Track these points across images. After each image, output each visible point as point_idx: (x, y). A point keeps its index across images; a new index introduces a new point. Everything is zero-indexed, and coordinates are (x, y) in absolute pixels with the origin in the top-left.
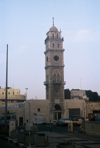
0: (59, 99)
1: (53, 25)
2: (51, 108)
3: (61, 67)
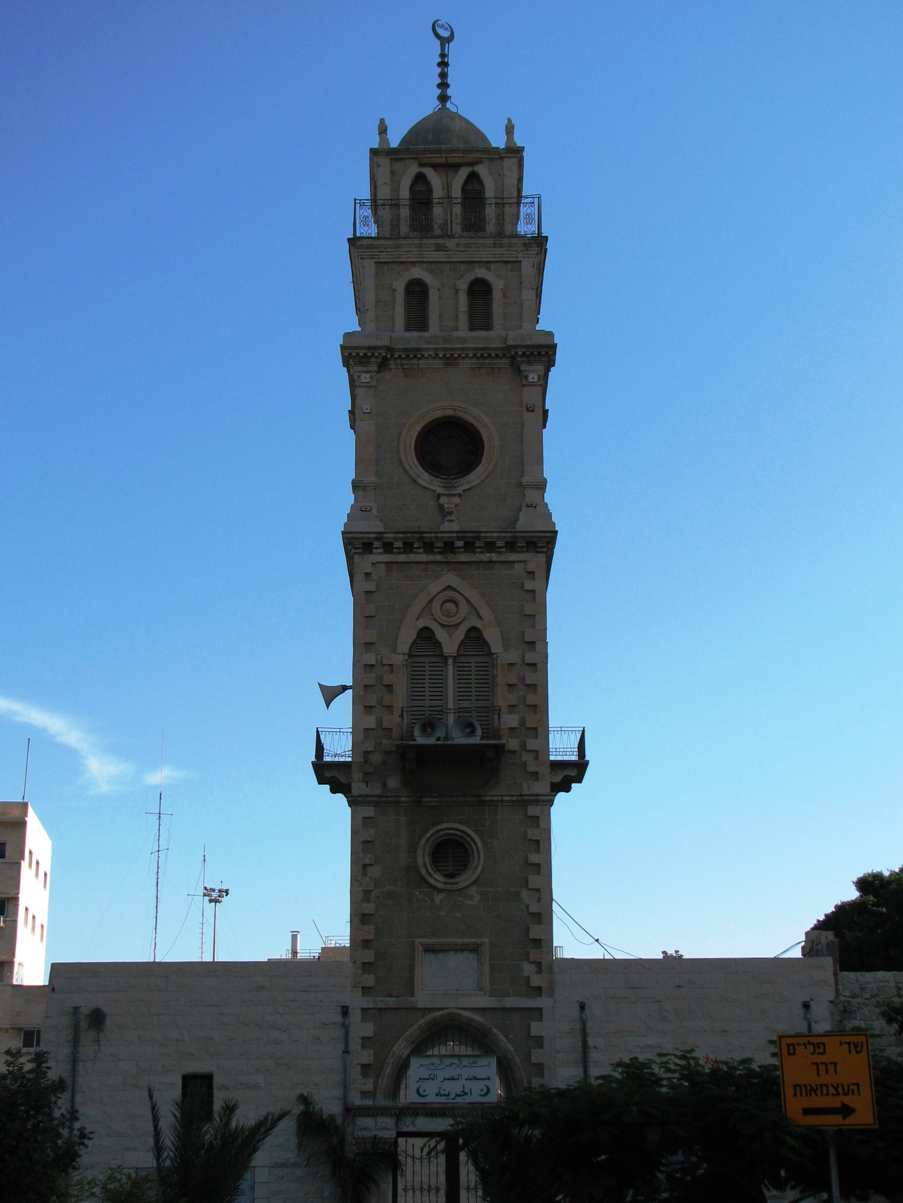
0: (475, 949)
1: (443, 98)
2: (365, 1067)
3: (511, 546)
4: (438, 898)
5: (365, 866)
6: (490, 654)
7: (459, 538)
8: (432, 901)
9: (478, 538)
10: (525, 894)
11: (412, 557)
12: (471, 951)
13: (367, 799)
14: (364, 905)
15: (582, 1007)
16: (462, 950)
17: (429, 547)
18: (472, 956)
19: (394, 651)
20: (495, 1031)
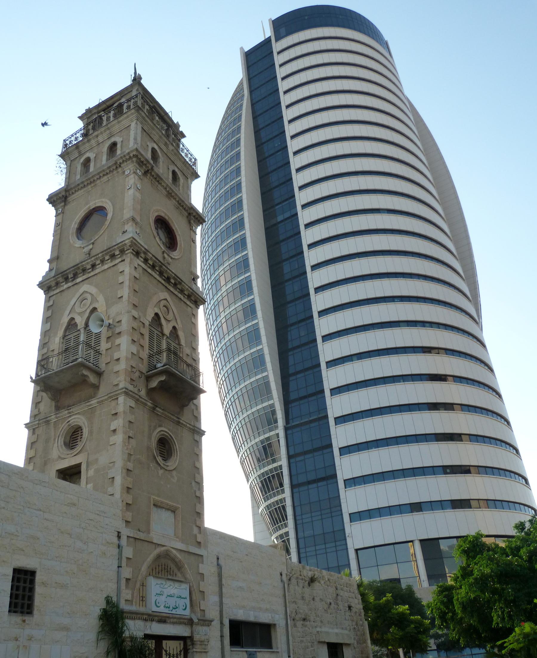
0: (174, 511)
4: (161, 472)
5: (129, 437)
6: (179, 344)
7: (174, 278)
8: (158, 472)
9: (180, 283)
10: (193, 483)
11: (153, 273)
12: (172, 511)
13: (134, 395)
14: (129, 463)
15: (218, 559)
16: (168, 509)
17: (161, 274)
18: (172, 515)
19: (145, 315)
20: (186, 566)
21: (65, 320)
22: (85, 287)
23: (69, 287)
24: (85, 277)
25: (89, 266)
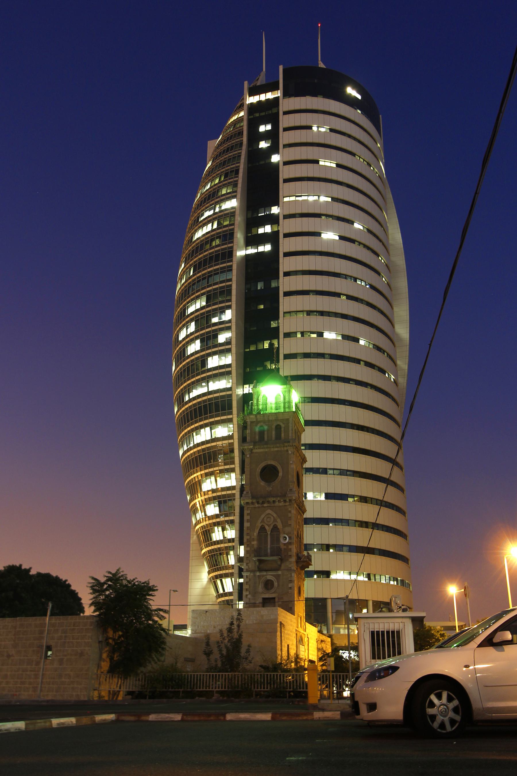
21: (259, 525)
22: (269, 511)
23: (259, 507)
24: (268, 505)
25: (271, 501)
